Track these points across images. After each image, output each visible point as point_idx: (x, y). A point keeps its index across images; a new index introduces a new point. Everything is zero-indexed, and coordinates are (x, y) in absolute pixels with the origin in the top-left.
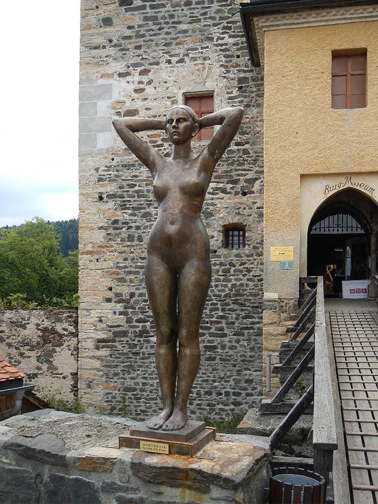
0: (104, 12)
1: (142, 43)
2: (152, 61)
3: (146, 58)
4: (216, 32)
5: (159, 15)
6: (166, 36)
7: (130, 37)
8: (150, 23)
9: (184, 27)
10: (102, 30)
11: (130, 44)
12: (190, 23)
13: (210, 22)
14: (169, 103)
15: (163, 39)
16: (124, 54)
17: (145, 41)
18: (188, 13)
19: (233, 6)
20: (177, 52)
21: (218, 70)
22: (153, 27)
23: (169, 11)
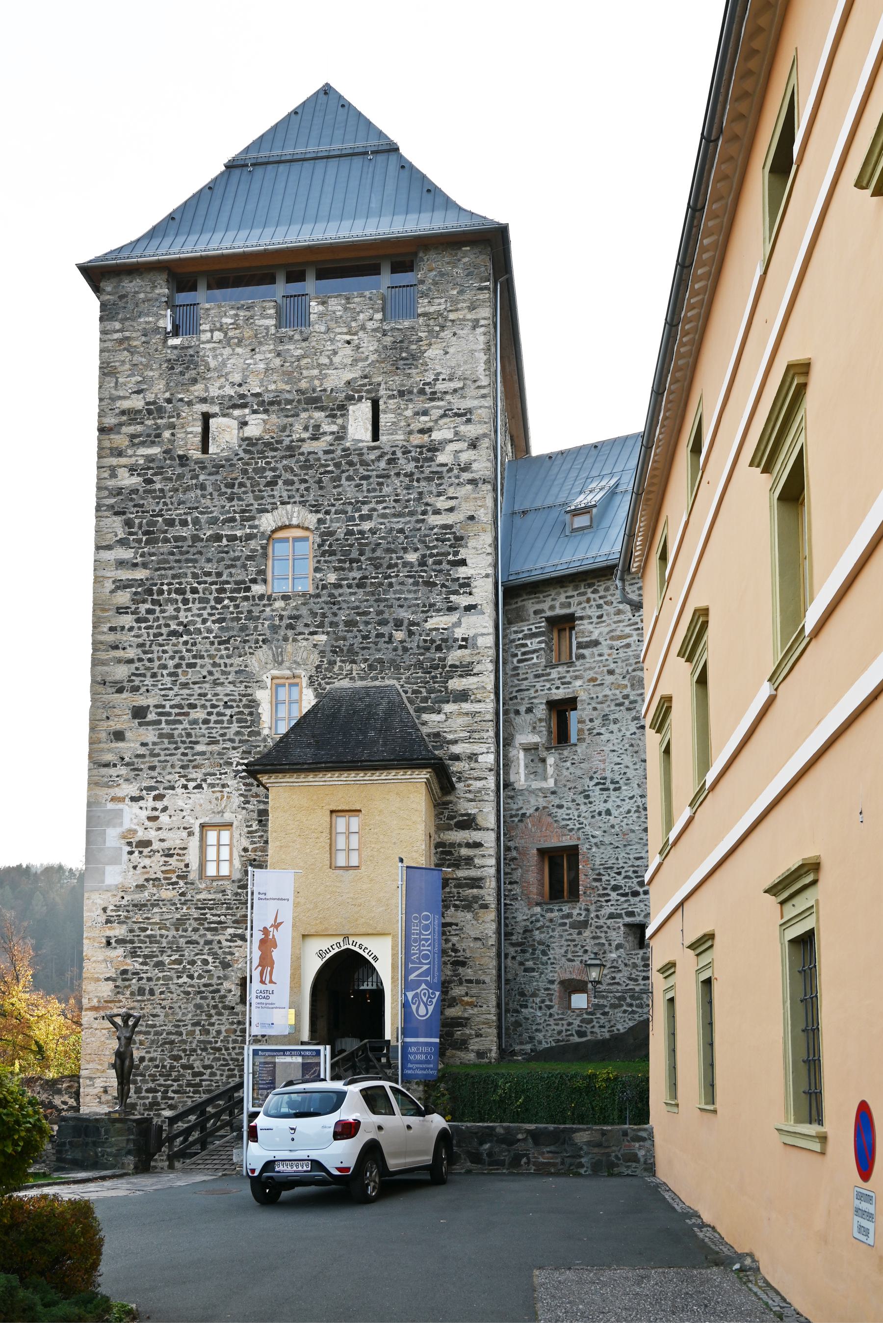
0: (115, 725)
1: (157, 764)
2: (167, 784)
3: (161, 782)
5: (176, 733)
6: (182, 758)
7: (143, 756)
8: (166, 741)
10: (114, 745)
11: (143, 763)
12: (208, 744)
13: (229, 745)
15: (179, 760)
16: (138, 775)
17: (159, 761)
18: (206, 732)
19: (253, 728)
20: (194, 776)
22: (169, 746)
23: (185, 729)
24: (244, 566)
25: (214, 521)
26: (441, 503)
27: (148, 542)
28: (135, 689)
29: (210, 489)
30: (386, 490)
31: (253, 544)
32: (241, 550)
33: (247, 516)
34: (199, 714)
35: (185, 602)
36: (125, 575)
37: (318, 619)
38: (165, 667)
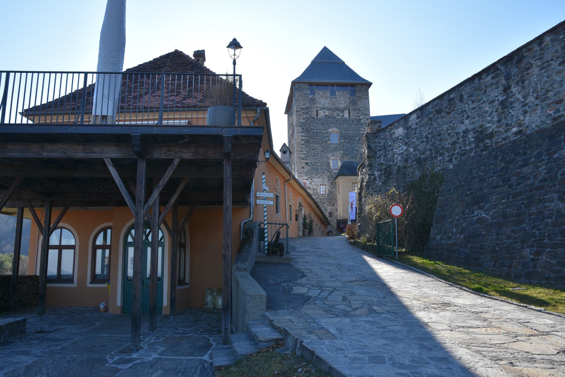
0: (302, 166)
4: (326, 172)
9: (319, 171)
14: (317, 186)
21: (327, 180)
24: (326, 138)
25: (320, 129)
26: (362, 129)
27: (307, 132)
28: (306, 159)
29: (319, 124)
30: (352, 126)
31: (328, 134)
32: (325, 135)
33: (326, 129)
34: (319, 164)
35: (315, 144)
36: (303, 138)
37: (341, 149)
38: (312, 155)
